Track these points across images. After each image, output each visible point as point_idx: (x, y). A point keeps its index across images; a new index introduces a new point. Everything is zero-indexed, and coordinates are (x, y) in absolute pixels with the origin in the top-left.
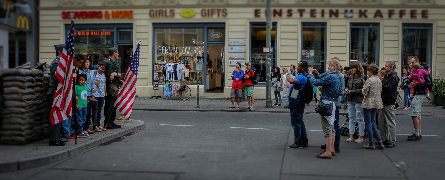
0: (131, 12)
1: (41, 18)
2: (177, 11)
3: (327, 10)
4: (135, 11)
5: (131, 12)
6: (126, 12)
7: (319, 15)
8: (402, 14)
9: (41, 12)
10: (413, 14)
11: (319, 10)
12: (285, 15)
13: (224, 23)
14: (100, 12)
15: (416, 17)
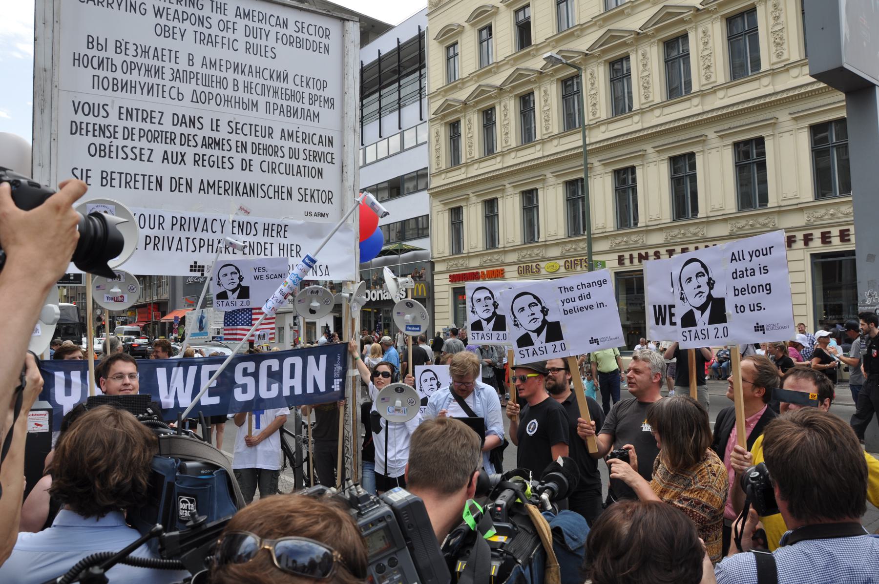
0: (502, 270)
1: (436, 283)
2: (542, 264)
3: (635, 254)
4: (507, 269)
5: (502, 270)
6: (497, 271)
7: (836, 241)
8: (807, 239)
9: (436, 277)
10: (825, 238)
11: (627, 255)
12: (652, 258)
13: (642, 270)
14: (477, 273)
15: (830, 242)
